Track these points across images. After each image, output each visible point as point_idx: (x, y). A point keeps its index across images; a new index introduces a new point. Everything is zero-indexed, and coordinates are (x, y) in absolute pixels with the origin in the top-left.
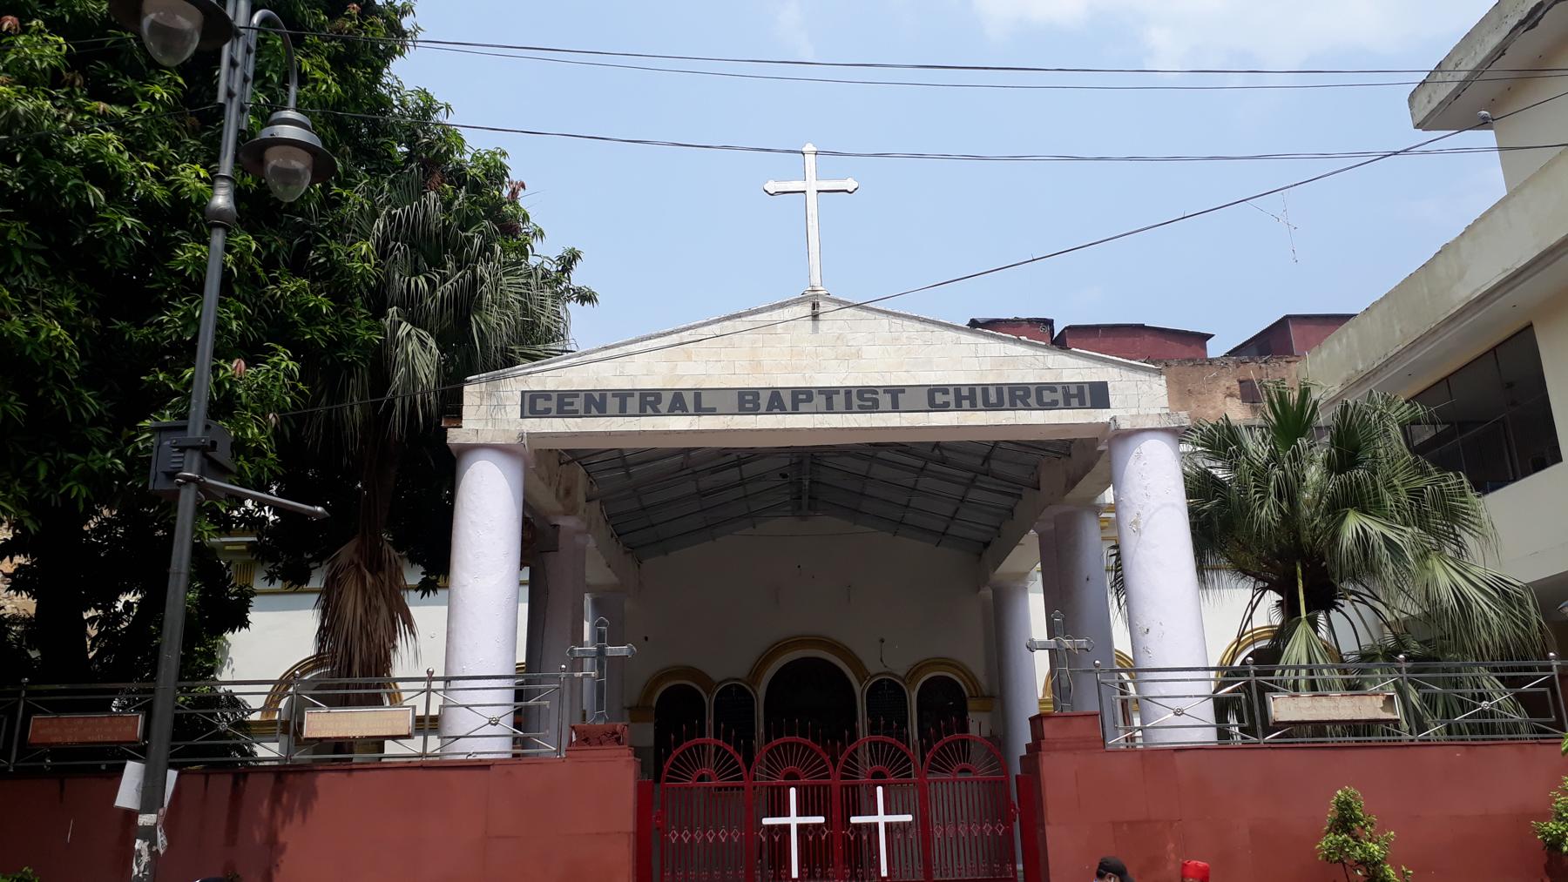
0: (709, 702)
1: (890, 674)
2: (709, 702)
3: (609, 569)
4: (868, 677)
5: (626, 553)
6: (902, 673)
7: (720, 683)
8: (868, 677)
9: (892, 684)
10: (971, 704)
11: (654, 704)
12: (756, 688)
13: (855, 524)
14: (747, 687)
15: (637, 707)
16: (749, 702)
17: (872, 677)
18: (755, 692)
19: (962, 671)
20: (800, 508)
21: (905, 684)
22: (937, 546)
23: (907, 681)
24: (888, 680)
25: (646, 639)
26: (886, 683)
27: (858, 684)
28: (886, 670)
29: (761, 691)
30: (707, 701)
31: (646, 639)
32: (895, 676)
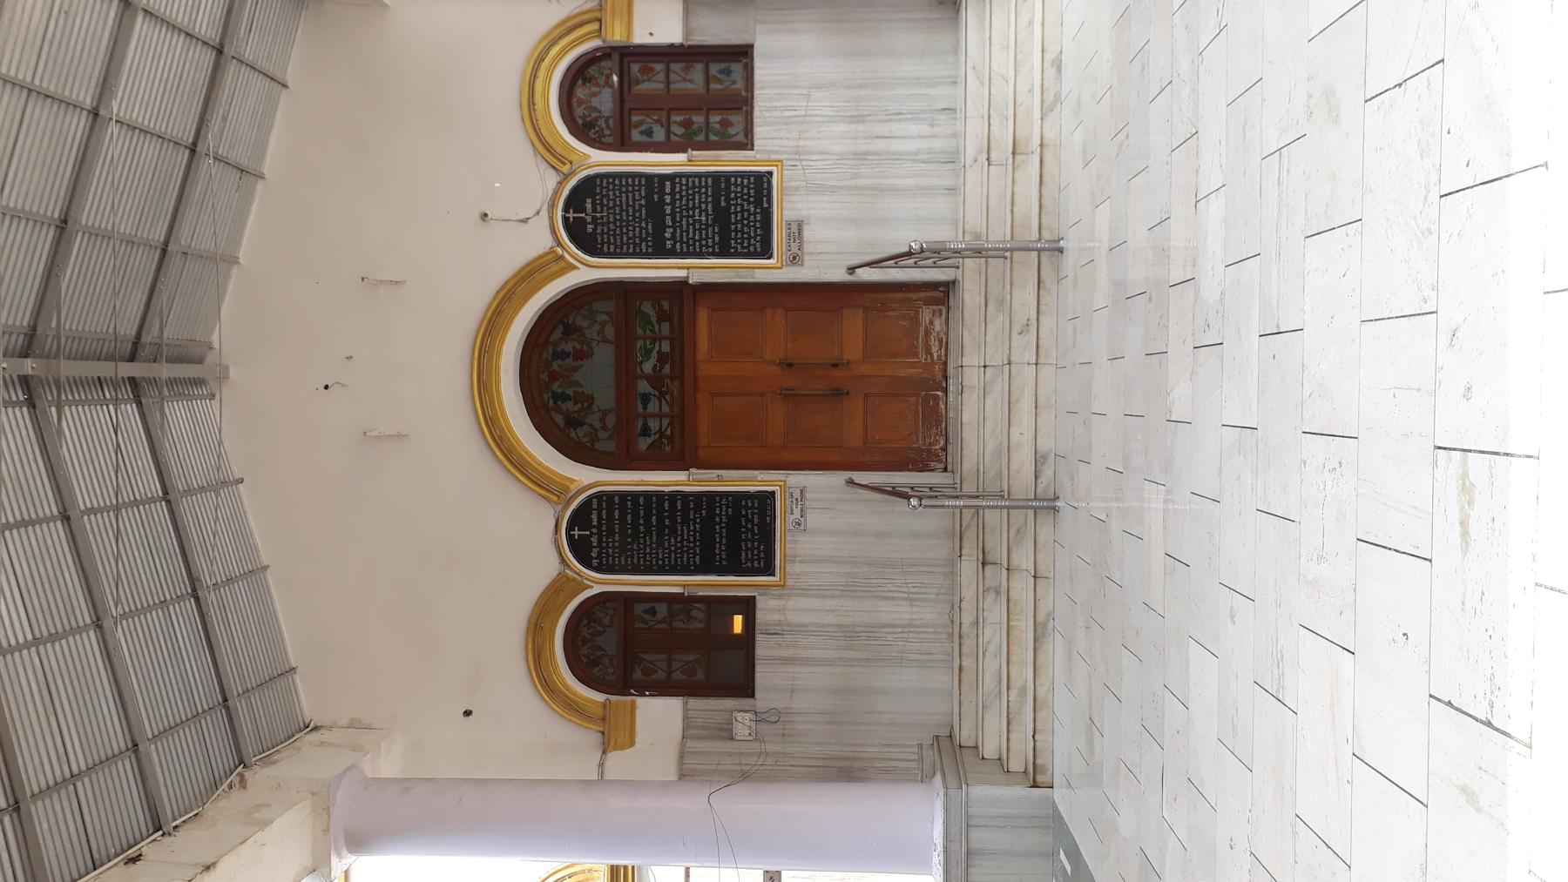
0: (600, 583)
1: (552, 206)
2: (600, 583)
3: (220, 867)
4: (559, 250)
5: (243, 782)
6: (552, 179)
7: (563, 560)
8: (559, 250)
9: (575, 201)
10: (616, 36)
11: (599, 697)
12: (574, 488)
13: (234, 261)
14: (574, 506)
15: (603, 733)
16: (604, 500)
17: (559, 244)
18: (590, 486)
19: (547, 50)
20: (199, 382)
21: (572, 173)
22: (285, 86)
23: (565, 169)
24: (566, 210)
25: (468, 713)
26: (571, 215)
27: (575, 272)
28: (544, 214)
29: (586, 478)
30: (597, 589)
31: (468, 713)
32: (557, 192)
